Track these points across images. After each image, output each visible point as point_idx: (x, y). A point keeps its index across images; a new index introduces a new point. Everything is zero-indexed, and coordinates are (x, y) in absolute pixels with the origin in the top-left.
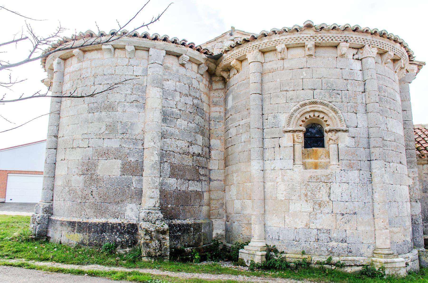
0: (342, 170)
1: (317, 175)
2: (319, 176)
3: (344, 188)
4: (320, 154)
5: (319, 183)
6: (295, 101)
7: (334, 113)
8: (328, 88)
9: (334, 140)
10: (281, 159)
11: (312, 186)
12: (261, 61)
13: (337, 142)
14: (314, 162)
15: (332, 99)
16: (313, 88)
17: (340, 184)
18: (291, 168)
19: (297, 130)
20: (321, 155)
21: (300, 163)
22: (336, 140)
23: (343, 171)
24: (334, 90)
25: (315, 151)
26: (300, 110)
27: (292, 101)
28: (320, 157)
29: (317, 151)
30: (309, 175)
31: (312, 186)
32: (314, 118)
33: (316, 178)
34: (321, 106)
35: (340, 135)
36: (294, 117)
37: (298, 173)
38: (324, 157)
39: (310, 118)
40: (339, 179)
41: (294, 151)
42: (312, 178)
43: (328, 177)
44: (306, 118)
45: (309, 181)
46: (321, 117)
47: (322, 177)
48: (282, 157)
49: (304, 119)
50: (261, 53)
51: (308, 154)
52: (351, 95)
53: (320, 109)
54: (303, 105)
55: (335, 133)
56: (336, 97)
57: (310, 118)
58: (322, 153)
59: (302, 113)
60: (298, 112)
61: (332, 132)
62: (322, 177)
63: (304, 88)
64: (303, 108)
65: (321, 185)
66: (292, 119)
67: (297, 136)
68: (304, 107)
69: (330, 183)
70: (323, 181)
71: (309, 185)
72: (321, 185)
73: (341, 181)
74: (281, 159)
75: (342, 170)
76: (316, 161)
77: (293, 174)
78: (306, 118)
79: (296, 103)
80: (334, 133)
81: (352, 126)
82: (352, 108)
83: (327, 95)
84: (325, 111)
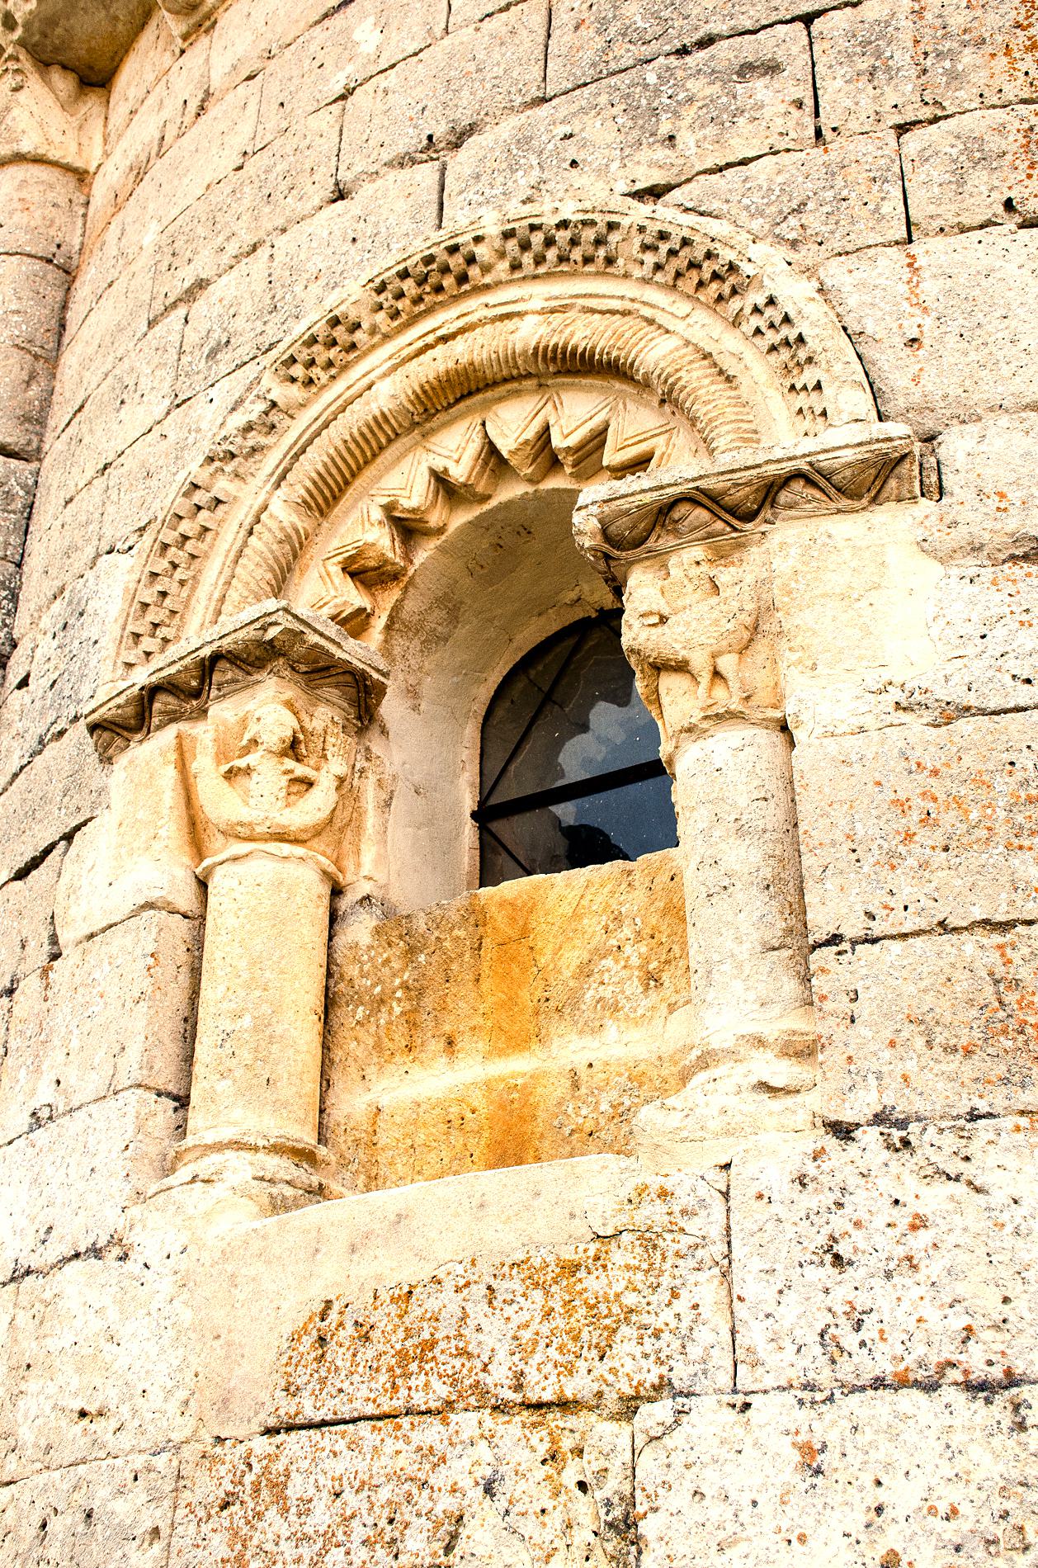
0: (842, 1131)
1: (412, 1272)
2: (447, 1301)
3: (902, 1496)
4: (572, 958)
5: (431, 1433)
6: (245, 352)
7: (701, 316)
8: (619, 49)
9: (699, 661)
10: (36, 1120)
11: (322, 1516)
12: (54, 154)
13: (760, 679)
14: (488, 1085)
15: (662, 153)
16: (440, 130)
17: (829, 1426)
18: (106, 1221)
19: (208, 667)
20: (585, 971)
21: (226, 1134)
22: (744, 649)
23: (870, 1136)
24: (707, 42)
25: (499, 918)
26: (294, 431)
27: (226, 359)
28: (574, 1000)
29: (539, 923)
30: (296, 1308)
31: (322, 1516)
32: (511, 491)
33: (389, 1340)
34: (538, 294)
35: (783, 565)
36: (228, 537)
37: (167, 1286)
38: (634, 987)
39: (461, 518)
40: (789, 1312)
41: (196, 972)
42: (338, 1355)
43: (593, 1283)
44: (407, 529)
45: (287, 1407)
46: (572, 441)
47: (478, 1310)
48: (46, 1094)
49: (382, 540)
50: (63, 83)
51: (415, 992)
52: (957, 21)
53: (529, 333)
54: (321, 354)
55: (721, 556)
56: (721, 119)
57: (461, 518)
58: (593, 925)
59: (315, 460)
60: (271, 461)
61: (659, 558)
62: (478, 1310)
63: (345, 176)
64: (328, 396)
65: (462, 1470)
66: (212, 572)
67: (221, 755)
68: (339, 387)
69: (629, 1408)
70: (499, 1377)
71: (279, 1489)
72: (462, 1470)
73: (833, 1349)
74: (36, 1120)
75: (842, 1131)
76: (519, 1065)
77: (113, 1314)
78: (407, 529)
79: (251, 371)
80: (688, 558)
81: (989, 390)
82: (979, 179)
83: (600, 133)
84: (581, 333)
